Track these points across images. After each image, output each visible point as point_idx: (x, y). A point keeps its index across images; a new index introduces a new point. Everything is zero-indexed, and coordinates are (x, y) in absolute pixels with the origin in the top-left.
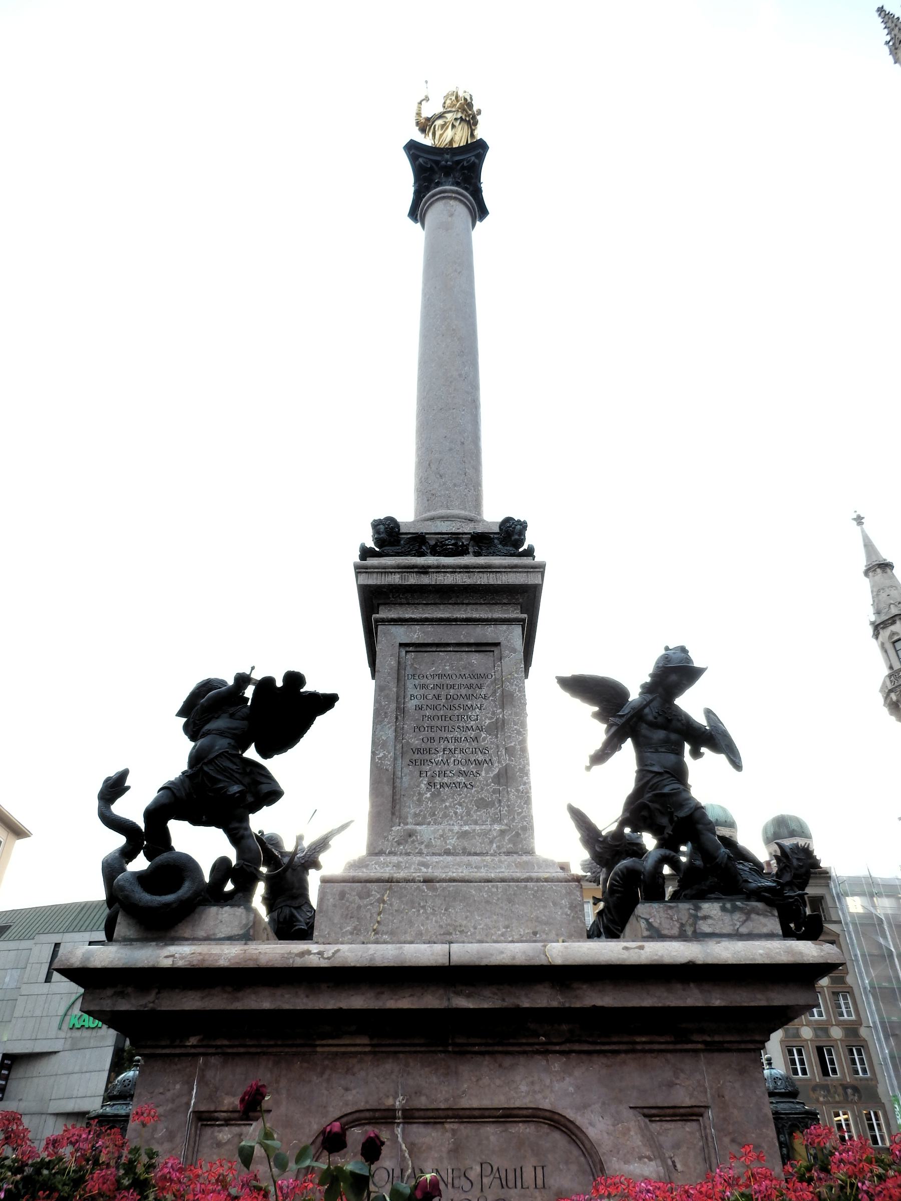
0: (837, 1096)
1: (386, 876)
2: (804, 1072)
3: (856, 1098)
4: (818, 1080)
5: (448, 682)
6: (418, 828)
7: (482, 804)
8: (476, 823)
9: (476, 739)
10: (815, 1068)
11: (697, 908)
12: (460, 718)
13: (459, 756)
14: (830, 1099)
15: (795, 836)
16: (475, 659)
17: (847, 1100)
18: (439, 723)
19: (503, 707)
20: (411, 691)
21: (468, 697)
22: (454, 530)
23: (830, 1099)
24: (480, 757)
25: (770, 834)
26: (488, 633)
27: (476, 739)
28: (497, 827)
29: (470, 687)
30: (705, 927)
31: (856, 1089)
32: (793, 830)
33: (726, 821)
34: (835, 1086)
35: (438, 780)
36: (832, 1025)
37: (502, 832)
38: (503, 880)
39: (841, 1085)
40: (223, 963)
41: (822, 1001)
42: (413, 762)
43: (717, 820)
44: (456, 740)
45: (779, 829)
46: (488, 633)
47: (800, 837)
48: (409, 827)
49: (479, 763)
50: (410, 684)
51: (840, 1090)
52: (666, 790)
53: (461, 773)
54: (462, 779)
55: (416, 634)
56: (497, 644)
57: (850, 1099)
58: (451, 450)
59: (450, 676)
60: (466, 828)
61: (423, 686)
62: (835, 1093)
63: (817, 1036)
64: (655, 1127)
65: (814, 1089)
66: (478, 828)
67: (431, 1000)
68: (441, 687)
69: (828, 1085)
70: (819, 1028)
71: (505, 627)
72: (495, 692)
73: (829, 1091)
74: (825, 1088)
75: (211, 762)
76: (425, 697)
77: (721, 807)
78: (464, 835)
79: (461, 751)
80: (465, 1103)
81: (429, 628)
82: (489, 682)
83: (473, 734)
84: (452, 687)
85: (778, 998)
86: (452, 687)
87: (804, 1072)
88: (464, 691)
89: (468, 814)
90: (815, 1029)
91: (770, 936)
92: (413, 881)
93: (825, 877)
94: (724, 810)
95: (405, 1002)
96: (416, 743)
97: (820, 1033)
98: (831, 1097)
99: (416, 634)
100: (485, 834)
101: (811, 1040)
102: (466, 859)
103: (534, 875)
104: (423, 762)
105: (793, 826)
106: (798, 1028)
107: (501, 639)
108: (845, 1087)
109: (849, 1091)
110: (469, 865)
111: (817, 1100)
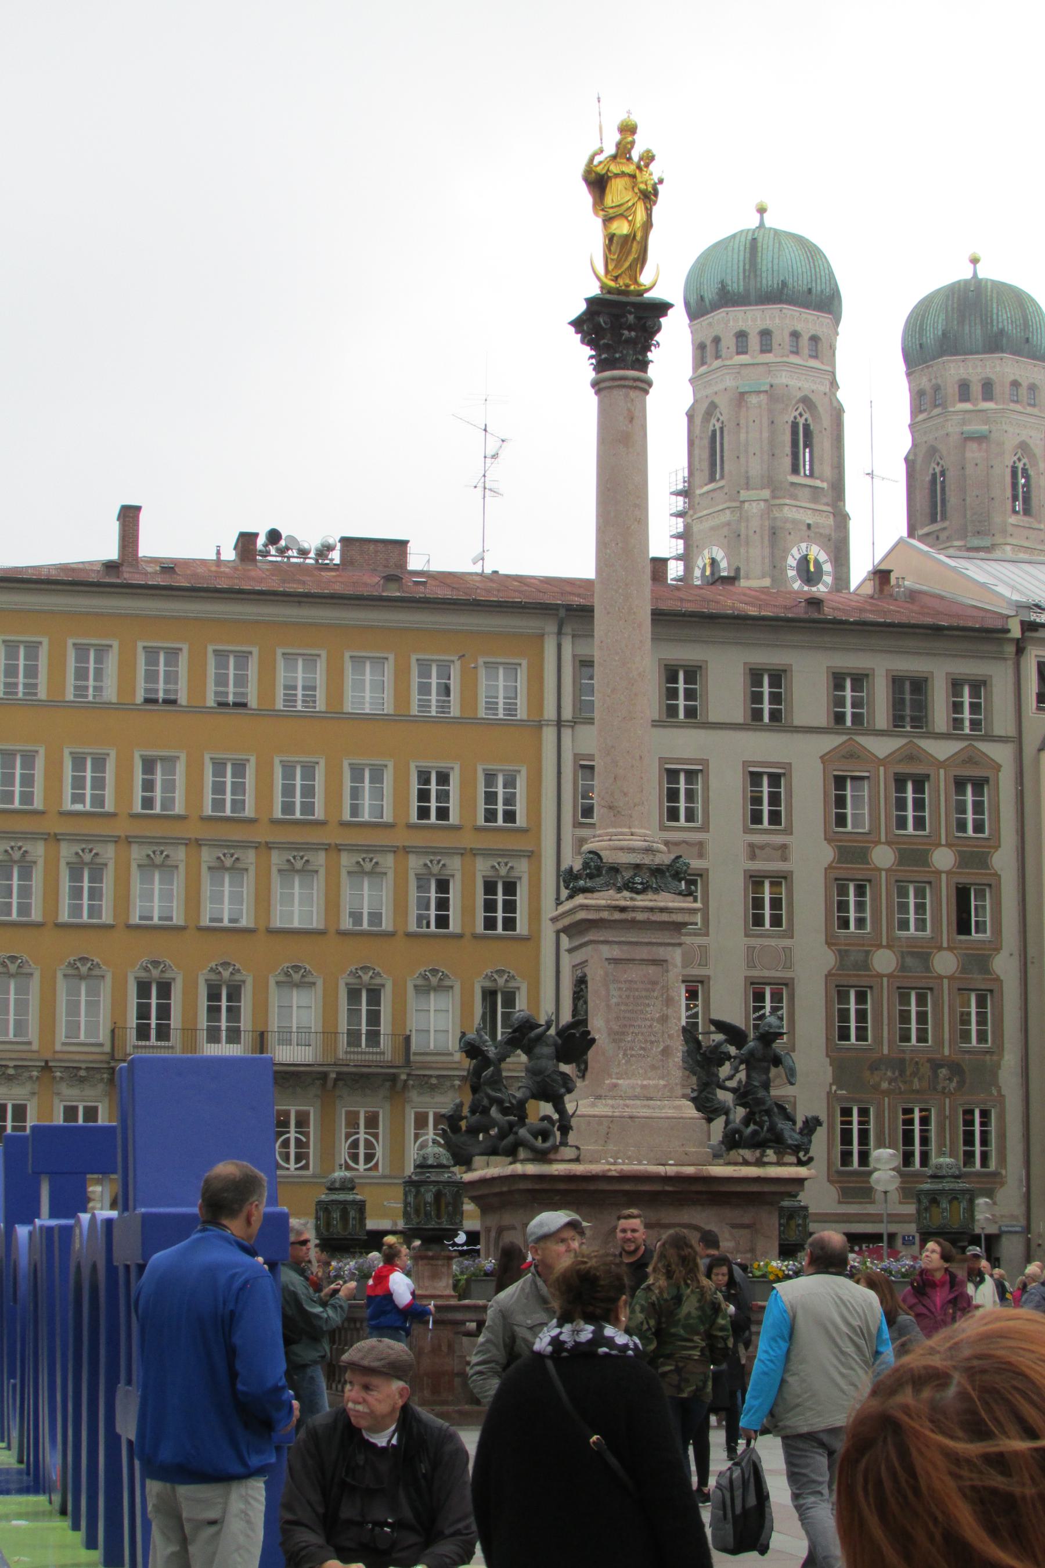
0: (916, 1080)
1: (610, 1114)
2: (861, 1035)
3: (954, 1085)
4: (886, 1051)
5: (635, 986)
6: (620, 1082)
7: (653, 1067)
8: (649, 1079)
9: (651, 1026)
10: (885, 1028)
11: (764, 1151)
12: (642, 1012)
13: (640, 1037)
14: (901, 1085)
15: (1003, 351)
16: (651, 970)
17: (935, 1089)
18: (627, 1015)
19: (667, 1006)
20: (613, 992)
21: (646, 997)
22: (638, 862)
23: (901, 1085)
24: (653, 1039)
25: (930, 337)
26: (661, 952)
27: (651, 1026)
28: (662, 1082)
29: (647, 990)
30: (765, 1159)
31: (956, 1069)
32: (1002, 332)
33: (810, 291)
34: (917, 1063)
35: (629, 1052)
36: (940, 948)
37: (665, 1086)
38: (668, 1118)
39: (929, 1060)
40: (578, 1173)
41: (932, 902)
42: (614, 1041)
43: (784, 284)
44: (640, 1027)
45: (961, 322)
46: (661, 952)
47: (1017, 352)
48: (614, 1081)
49: (652, 1042)
50: (612, 987)
51: (926, 1070)
52: (759, 1096)
53: (642, 1048)
54: (642, 1052)
55: (616, 952)
56: (666, 961)
57: (939, 1087)
58: (632, 766)
59: (636, 982)
60: (645, 1083)
61: (620, 989)
62: (914, 1074)
63: (903, 967)
64: (735, 1231)
65: (874, 1067)
66: (651, 1082)
67: (657, 1187)
68: (628, 989)
69: (902, 1061)
70: (912, 954)
71: (670, 948)
72: (662, 995)
73: (902, 1072)
74: (899, 1065)
75: (548, 1076)
76: (620, 997)
77: (801, 242)
78: (643, 1087)
79: (642, 1034)
80: (663, 1221)
81: (625, 948)
82: (659, 987)
83: (648, 1023)
84: (637, 990)
85: (789, 1188)
86: (637, 990)
87: (861, 1035)
88: (644, 993)
89: (646, 1072)
90: (903, 955)
91: (791, 1164)
92: (624, 1117)
93: (998, 639)
94: (812, 252)
95: (647, 1187)
96: (616, 1028)
97: (909, 961)
98: (905, 1082)
99: (616, 952)
100: (656, 1086)
101: (890, 976)
102: (646, 1102)
103: (684, 1115)
104: (621, 1040)
105: (1004, 318)
106: (867, 953)
107: (668, 958)
108: (936, 1065)
109: (943, 1072)
110: (649, 1107)
111: (876, 1087)
